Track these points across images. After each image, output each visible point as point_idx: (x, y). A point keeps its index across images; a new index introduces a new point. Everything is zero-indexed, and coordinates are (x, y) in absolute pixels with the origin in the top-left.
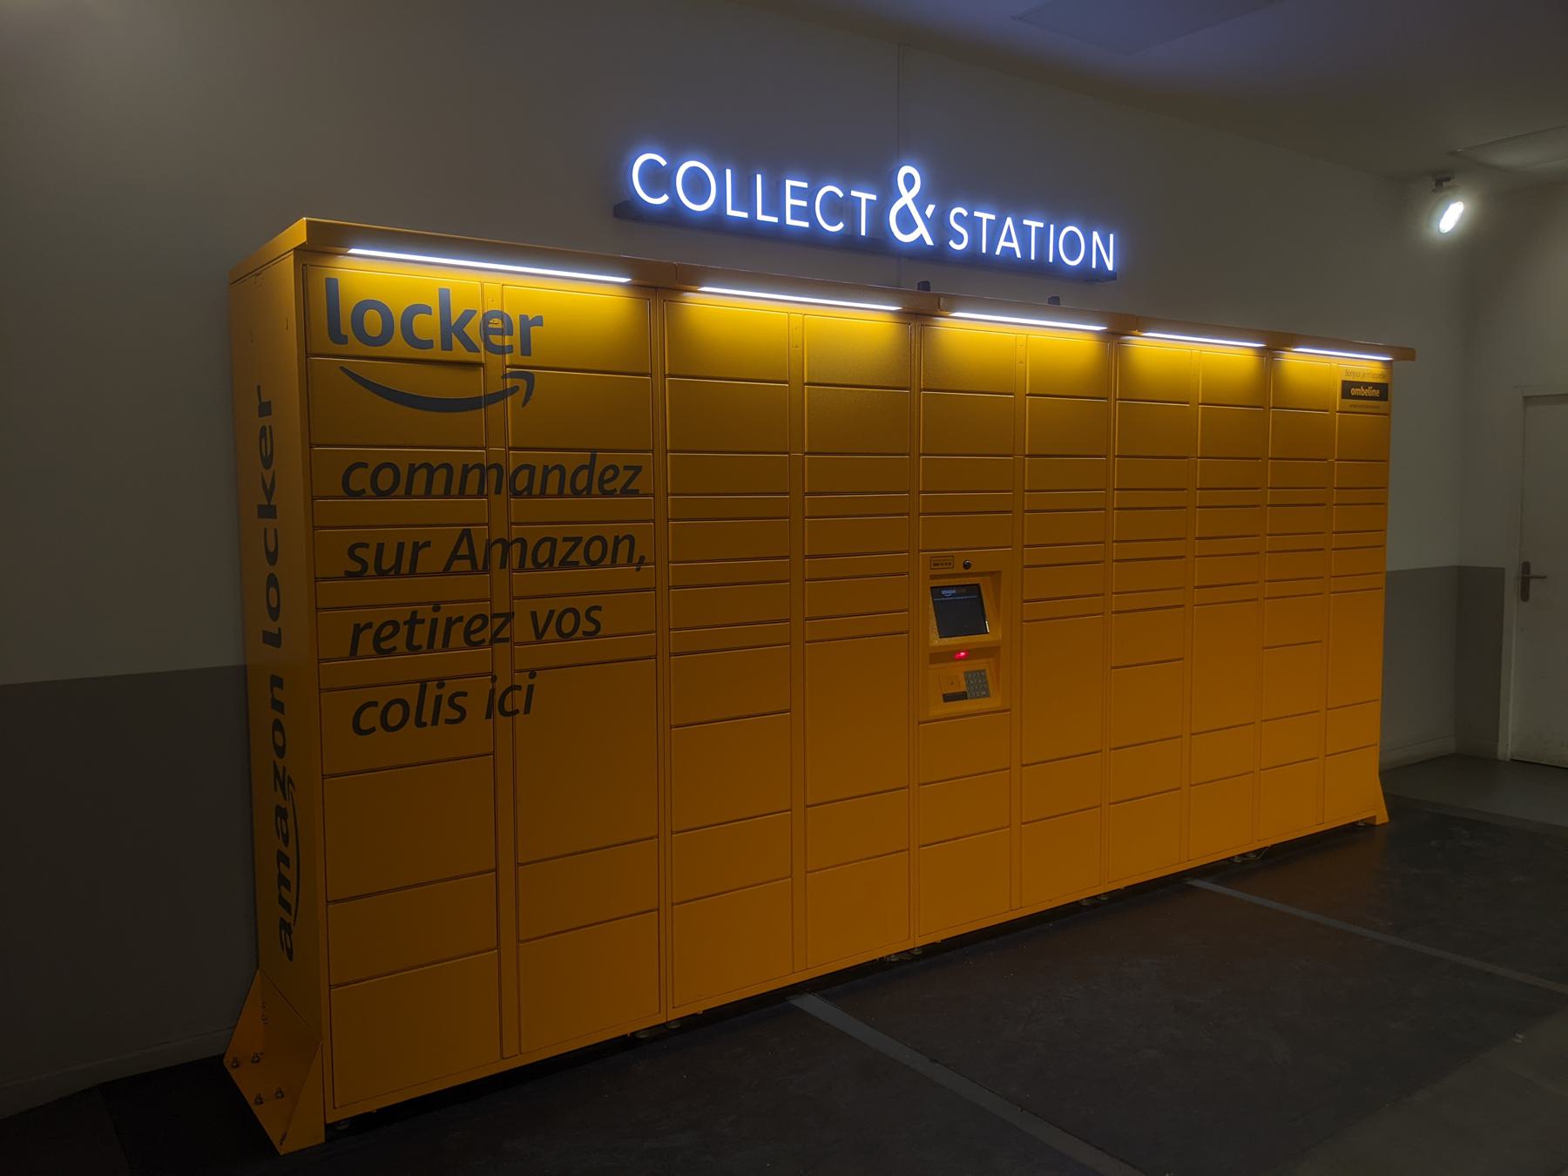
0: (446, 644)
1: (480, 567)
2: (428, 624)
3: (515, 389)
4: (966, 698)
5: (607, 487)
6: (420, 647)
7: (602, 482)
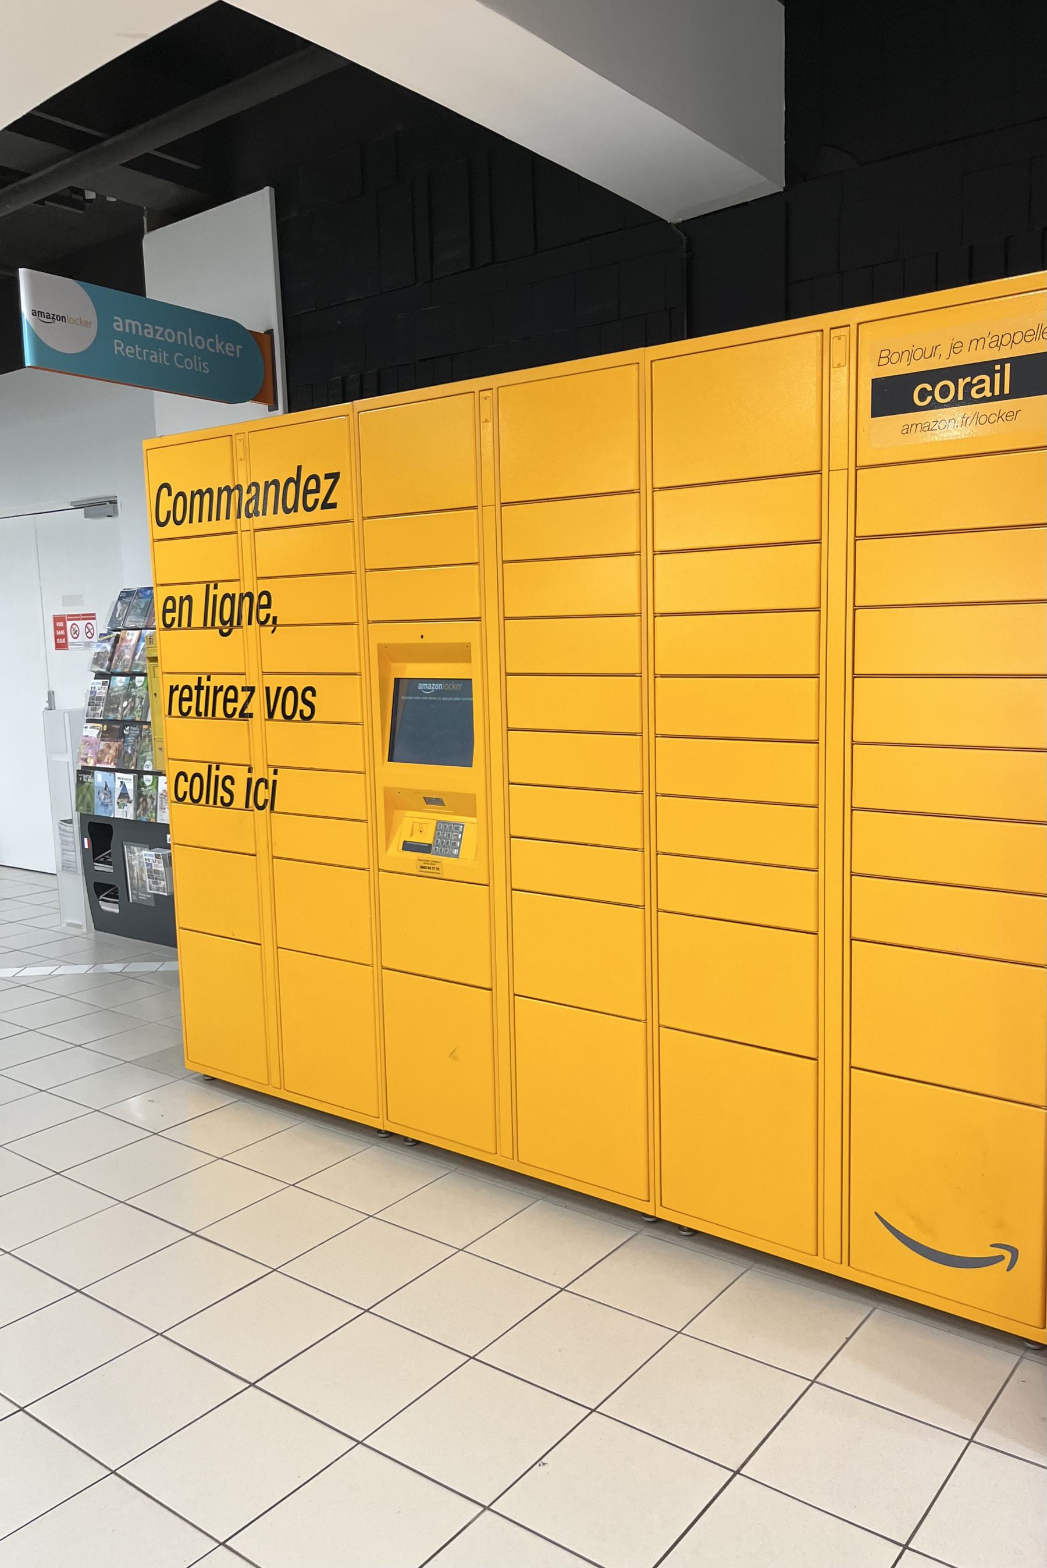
0: (214, 714)
2: (205, 688)
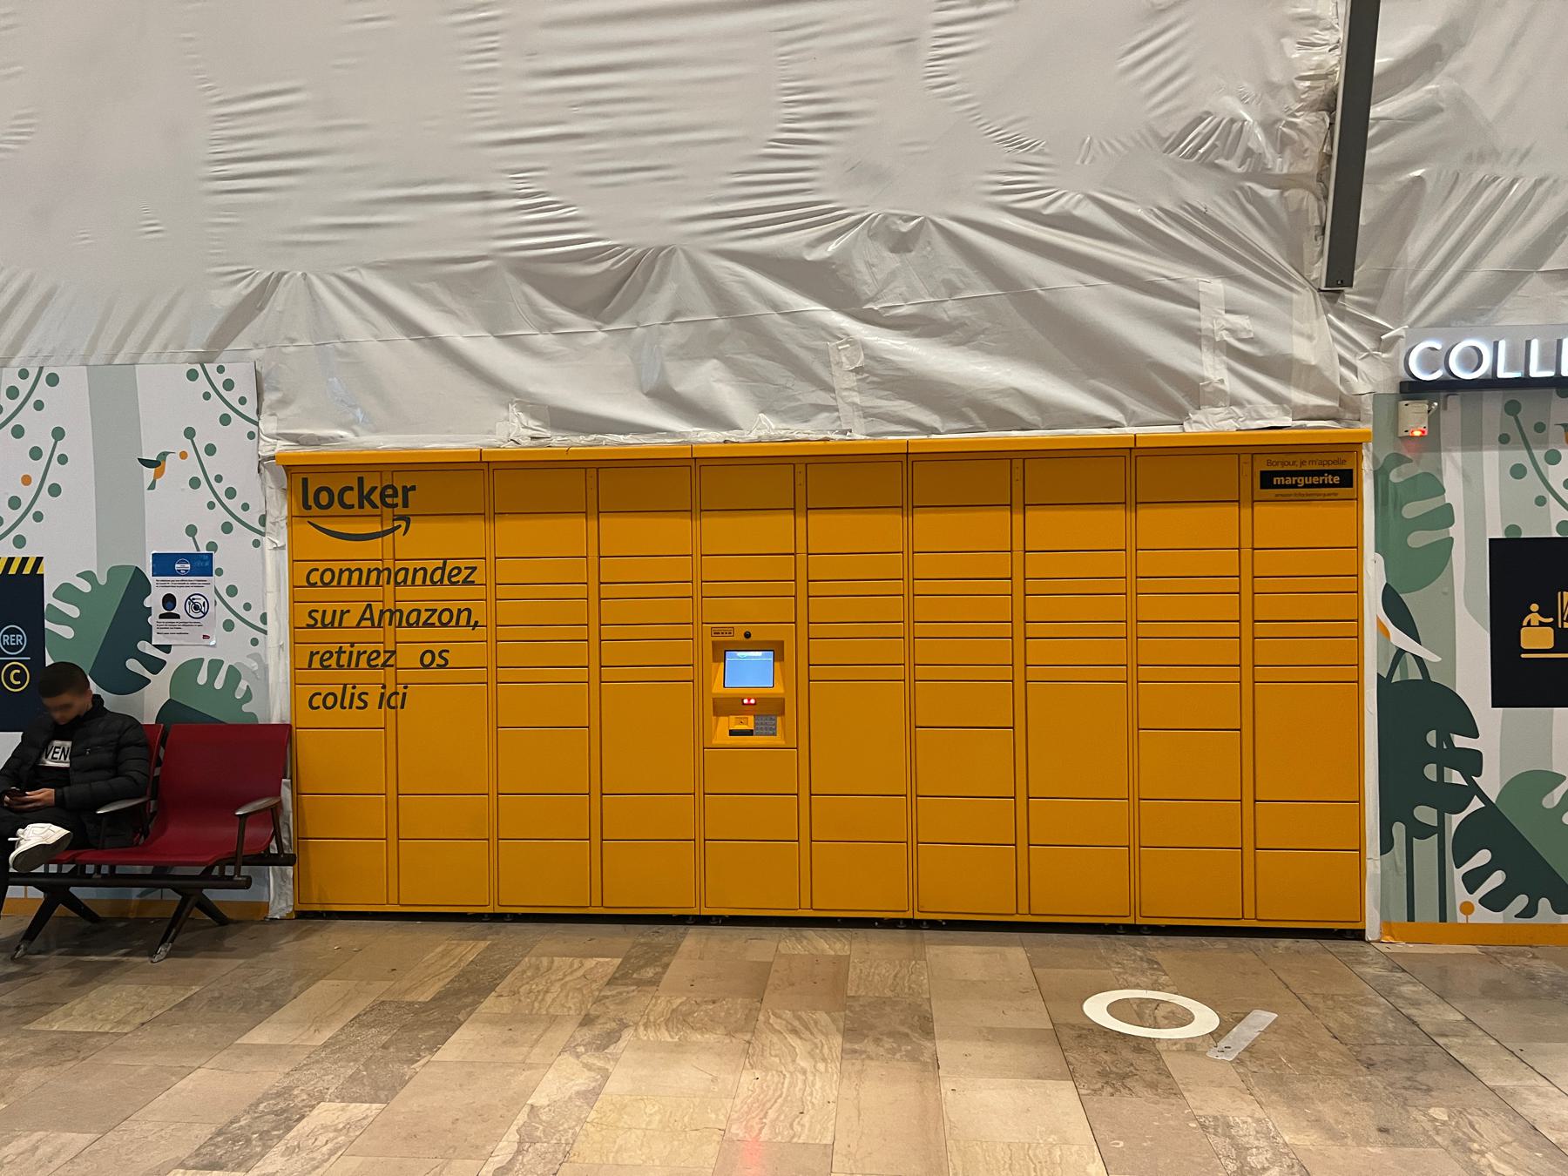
0: (357, 665)
1: (376, 625)
2: (348, 653)
3: (400, 526)
4: (752, 735)
5: (453, 579)
6: (343, 666)
7: (450, 577)
